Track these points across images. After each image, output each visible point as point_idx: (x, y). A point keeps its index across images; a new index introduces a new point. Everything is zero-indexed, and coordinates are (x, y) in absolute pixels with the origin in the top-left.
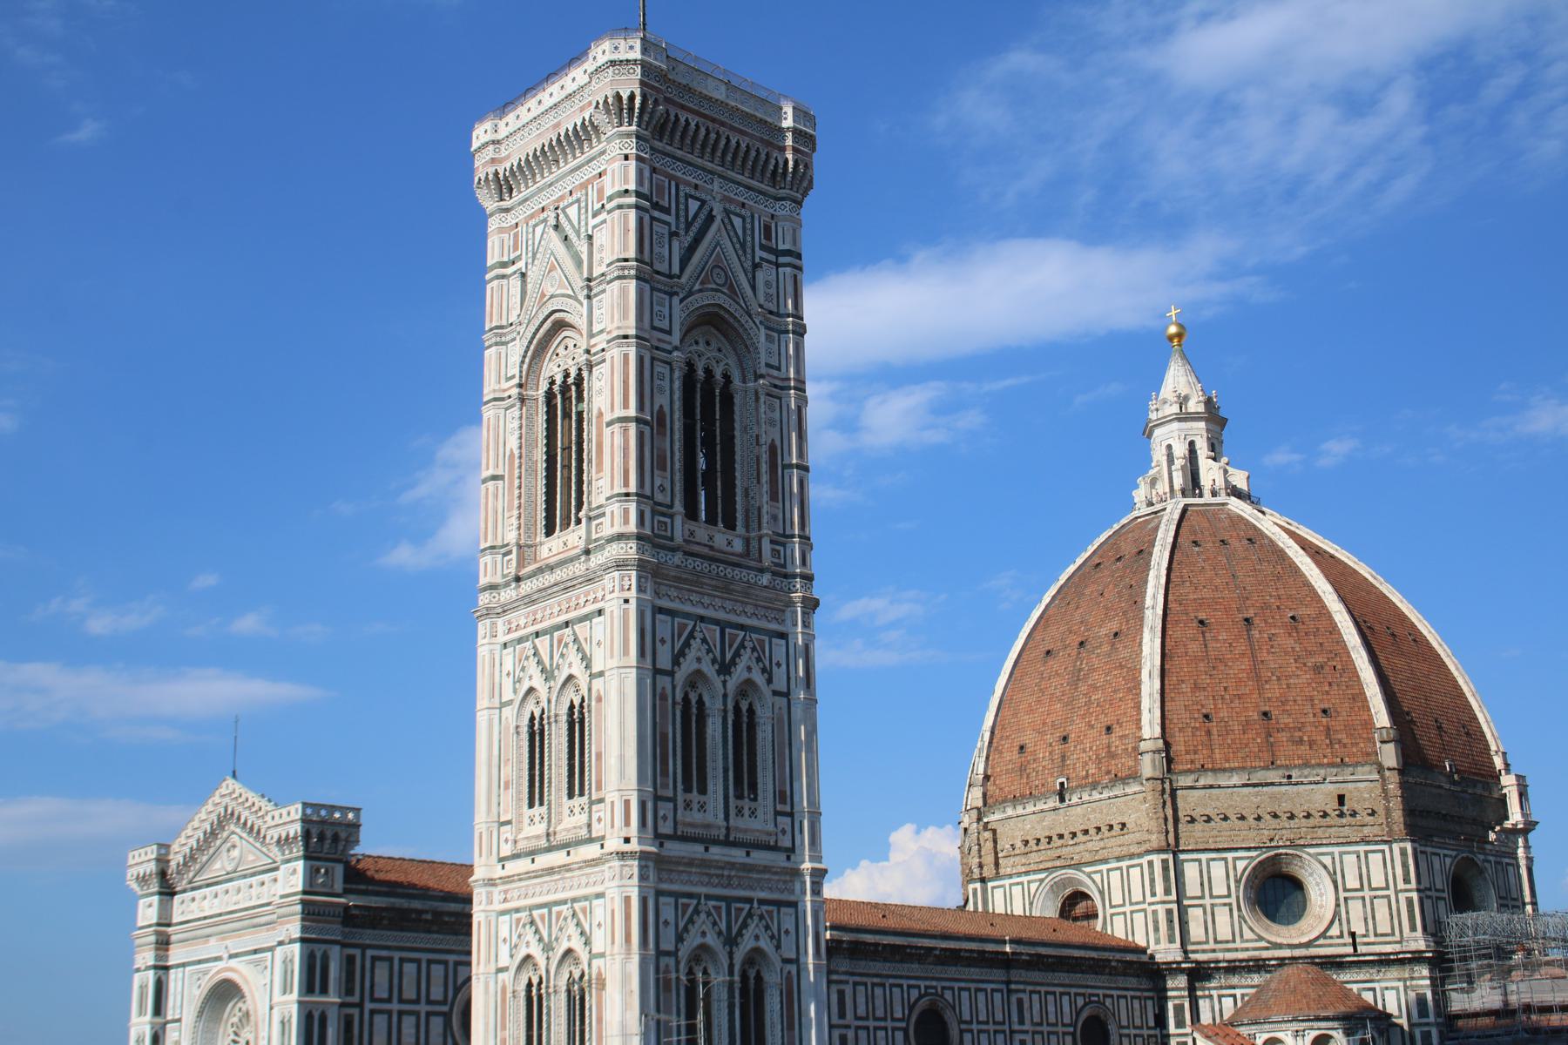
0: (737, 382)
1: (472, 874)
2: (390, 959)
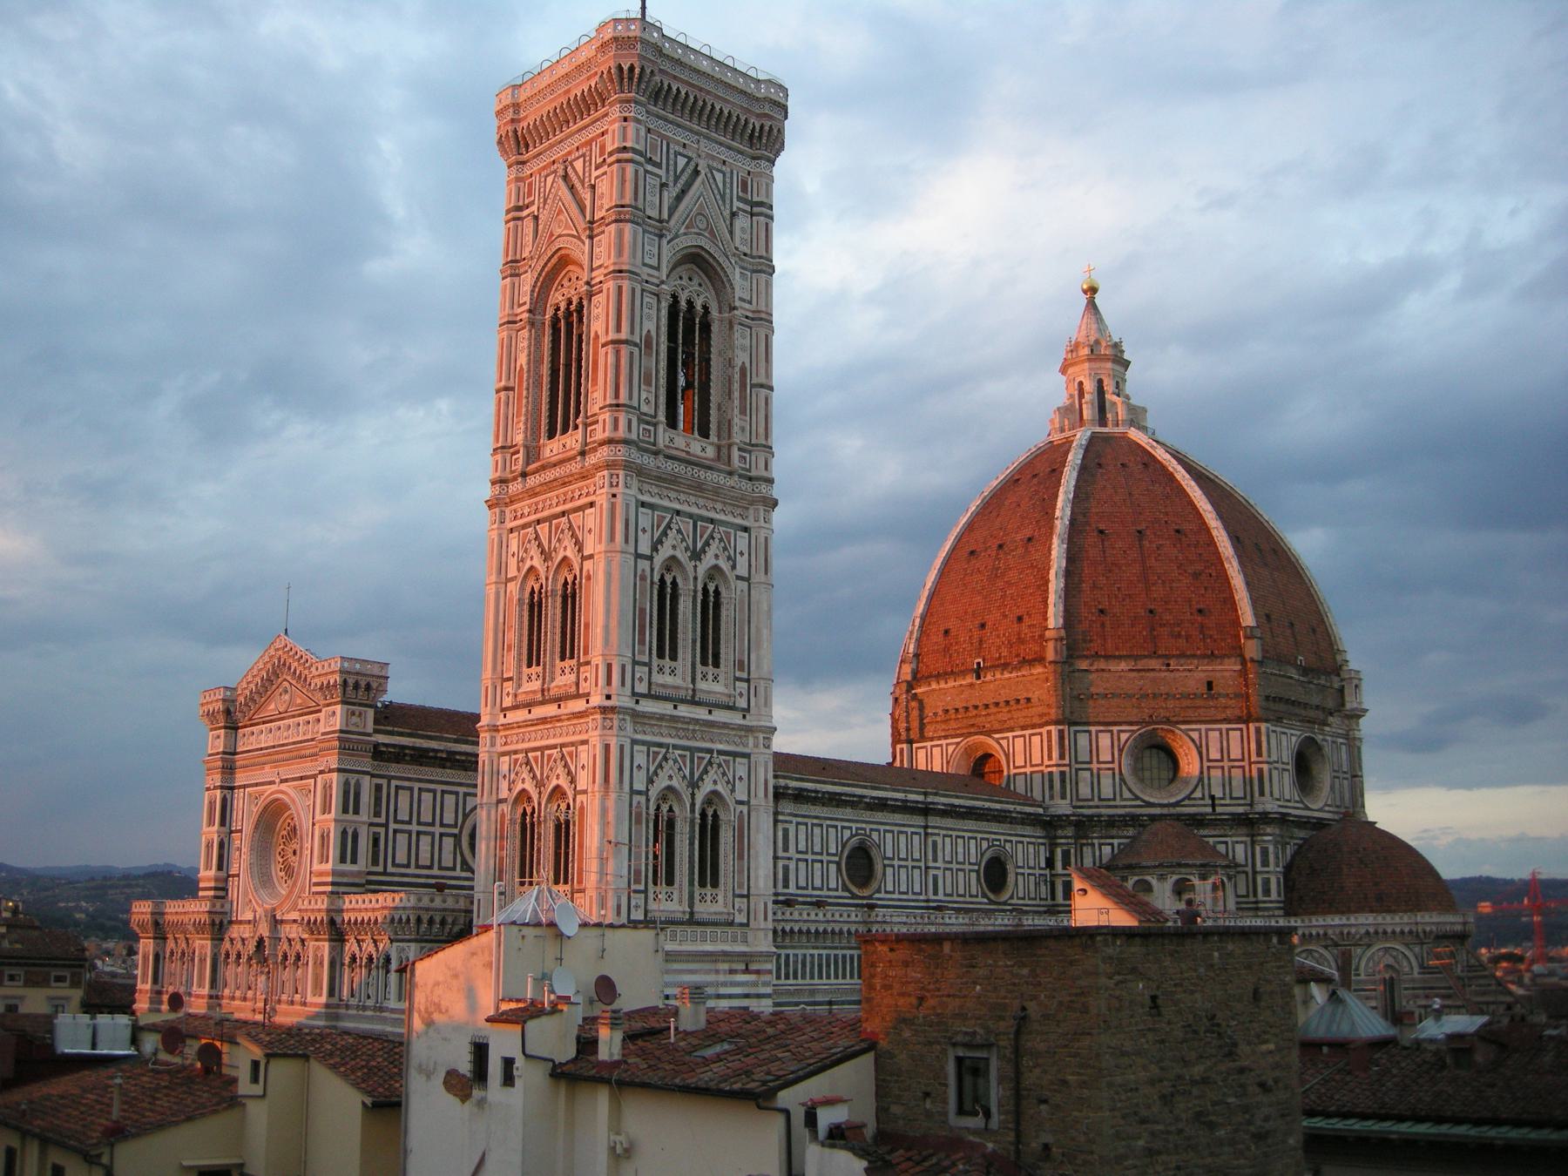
0: (714, 313)
1: (479, 721)
2: (411, 789)
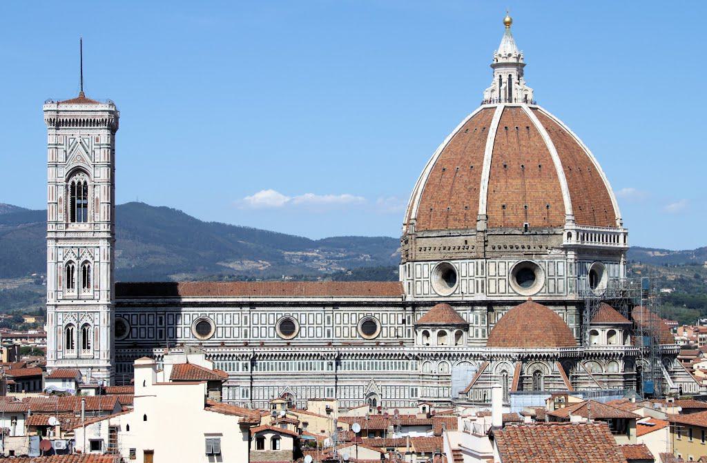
0: (88, 183)
